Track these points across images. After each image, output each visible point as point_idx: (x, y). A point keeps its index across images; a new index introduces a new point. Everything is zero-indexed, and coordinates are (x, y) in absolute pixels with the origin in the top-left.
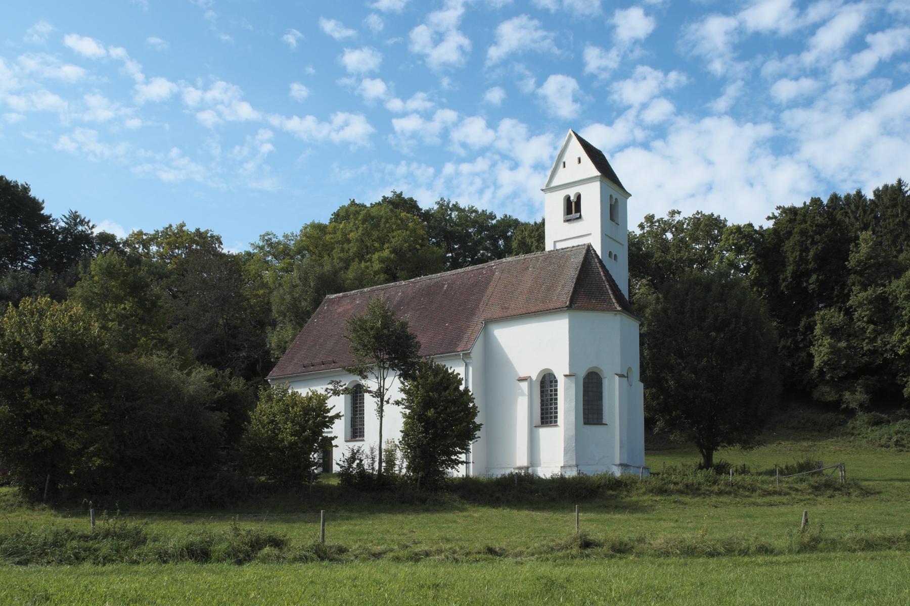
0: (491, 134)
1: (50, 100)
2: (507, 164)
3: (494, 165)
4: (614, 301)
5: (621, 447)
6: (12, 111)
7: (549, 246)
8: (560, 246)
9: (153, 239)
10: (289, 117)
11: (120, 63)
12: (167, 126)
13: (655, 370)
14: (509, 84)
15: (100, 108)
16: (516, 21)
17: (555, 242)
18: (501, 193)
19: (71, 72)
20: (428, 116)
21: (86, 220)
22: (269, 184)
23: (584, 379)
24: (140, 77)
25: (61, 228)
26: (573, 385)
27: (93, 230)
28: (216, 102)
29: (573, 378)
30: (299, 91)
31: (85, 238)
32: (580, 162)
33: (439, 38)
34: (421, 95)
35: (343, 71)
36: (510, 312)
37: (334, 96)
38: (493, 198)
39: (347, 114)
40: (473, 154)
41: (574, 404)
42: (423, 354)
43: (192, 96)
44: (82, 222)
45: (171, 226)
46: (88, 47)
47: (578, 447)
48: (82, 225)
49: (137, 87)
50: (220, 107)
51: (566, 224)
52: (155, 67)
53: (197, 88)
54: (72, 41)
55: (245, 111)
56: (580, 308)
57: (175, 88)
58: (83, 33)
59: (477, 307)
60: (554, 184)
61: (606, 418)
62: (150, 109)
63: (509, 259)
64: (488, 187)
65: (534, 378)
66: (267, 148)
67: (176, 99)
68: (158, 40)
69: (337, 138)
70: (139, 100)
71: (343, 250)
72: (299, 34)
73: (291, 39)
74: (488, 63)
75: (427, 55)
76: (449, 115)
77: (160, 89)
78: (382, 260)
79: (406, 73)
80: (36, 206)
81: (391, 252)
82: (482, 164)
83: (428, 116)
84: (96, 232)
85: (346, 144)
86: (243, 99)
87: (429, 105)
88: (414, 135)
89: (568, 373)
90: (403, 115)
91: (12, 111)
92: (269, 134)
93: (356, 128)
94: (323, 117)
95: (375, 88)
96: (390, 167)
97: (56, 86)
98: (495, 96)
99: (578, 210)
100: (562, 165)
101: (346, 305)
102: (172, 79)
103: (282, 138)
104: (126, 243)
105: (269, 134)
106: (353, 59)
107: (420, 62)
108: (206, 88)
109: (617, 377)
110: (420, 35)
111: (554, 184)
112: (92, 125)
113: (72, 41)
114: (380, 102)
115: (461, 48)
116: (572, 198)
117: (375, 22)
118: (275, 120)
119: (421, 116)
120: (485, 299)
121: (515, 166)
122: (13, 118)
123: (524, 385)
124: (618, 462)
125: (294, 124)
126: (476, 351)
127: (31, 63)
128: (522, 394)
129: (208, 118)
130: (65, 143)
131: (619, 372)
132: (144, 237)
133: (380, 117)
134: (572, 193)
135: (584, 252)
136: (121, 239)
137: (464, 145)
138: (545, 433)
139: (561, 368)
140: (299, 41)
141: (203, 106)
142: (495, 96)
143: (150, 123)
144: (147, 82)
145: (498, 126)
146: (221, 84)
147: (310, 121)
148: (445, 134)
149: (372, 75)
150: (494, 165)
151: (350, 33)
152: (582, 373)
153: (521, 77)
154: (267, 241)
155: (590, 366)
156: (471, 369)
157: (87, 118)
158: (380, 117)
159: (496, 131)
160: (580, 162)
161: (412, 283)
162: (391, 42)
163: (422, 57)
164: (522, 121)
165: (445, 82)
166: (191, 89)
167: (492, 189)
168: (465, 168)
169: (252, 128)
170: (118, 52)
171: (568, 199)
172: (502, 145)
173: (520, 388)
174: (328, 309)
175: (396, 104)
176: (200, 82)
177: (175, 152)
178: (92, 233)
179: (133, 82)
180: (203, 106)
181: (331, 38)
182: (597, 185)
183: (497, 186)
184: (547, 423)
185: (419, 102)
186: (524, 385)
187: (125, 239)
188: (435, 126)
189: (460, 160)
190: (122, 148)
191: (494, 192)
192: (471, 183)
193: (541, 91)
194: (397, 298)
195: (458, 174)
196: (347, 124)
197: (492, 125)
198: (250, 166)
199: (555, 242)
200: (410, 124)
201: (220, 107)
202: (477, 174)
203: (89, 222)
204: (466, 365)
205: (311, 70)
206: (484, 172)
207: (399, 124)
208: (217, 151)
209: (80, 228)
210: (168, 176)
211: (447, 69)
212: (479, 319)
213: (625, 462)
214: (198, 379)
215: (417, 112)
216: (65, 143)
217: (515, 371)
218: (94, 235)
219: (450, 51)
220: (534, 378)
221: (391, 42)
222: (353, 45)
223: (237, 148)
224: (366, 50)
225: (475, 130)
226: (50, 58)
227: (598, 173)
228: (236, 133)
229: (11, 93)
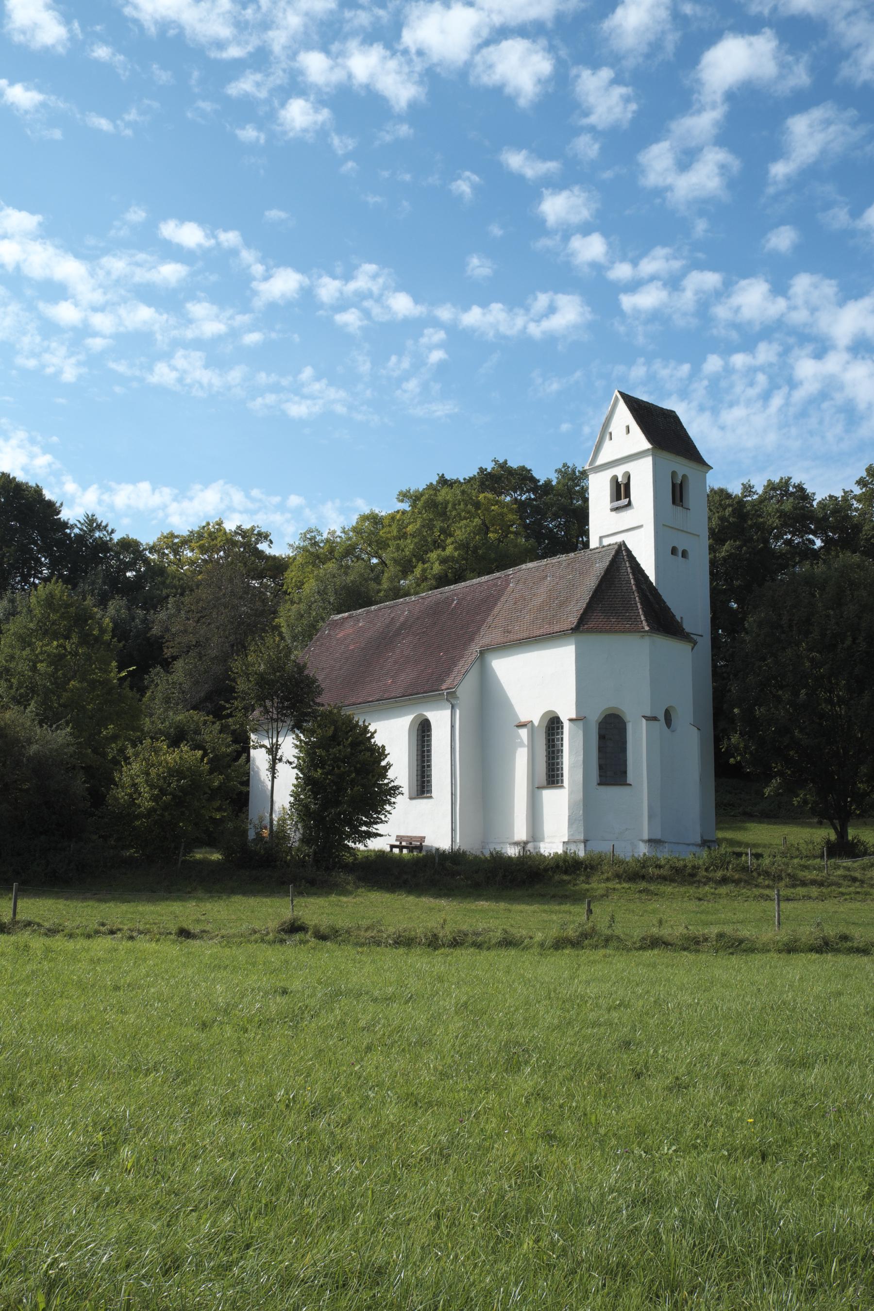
0: (781, 304)
1: (143, 315)
2: (809, 348)
3: (786, 351)
4: (643, 618)
5: (650, 817)
6: (95, 334)
7: (594, 543)
8: (606, 542)
9: (185, 542)
10: (466, 309)
11: (234, 252)
12: (296, 338)
13: (724, 711)
14: (804, 218)
15: (207, 320)
16: (817, 114)
17: (601, 538)
18: (799, 395)
19: (171, 272)
20: (673, 283)
21: (104, 524)
22: (441, 409)
23: (600, 724)
24: (258, 269)
25: (76, 535)
26: (581, 733)
27: (113, 536)
28: (362, 296)
29: (581, 723)
30: (478, 266)
31: (103, 546)
32: (628, 431)
33: (686, 159)
34: (660, 252)
35: (539, 227)
36: (512, 637)
37: (534, 268)
38: (787, 404)
39: (550, 294)
40: (749, 337)
41: (581, 758)
42: (326, 701)
43: (328, 289)
44: (99, 527)
45: (208, 524)
46: (190, 235)
47: (587, 814)
48: (100, 530)
49: (254, 284)
50: (367, 304)
51: (614, 513)
52: (278, 255)
53: (334, 277)
54: (170, 230)
55: (402, 304)
56: (590, 631)
57: (307, 281)
58: (183, 218)
59: (479, 629)
60: (600, 461)
61: (631, 777)
62: (276, 312)
63: (530, 565)
64: (779, 388)
65: (536, 723)
66: (437, 356)
67: (307, 294)
68: (283, 215)
69: (535, 330)
70: (258, 303)
71: (398, 548)
72: (475, 178)
73: (463, 187)
74: (771, 190)
75: (670, 188)
76: (711, 279)
77: (284, 283)
78: (443, 561)
79: (636, 219)
80: (51, 508)
81: (456, 549)
82: (766, 353)
83: (673, 283)
84: (116, 537)
85: (551, 339)
86: (399, 288)
87: (676, 265)
88: (656, 316)
89: (574, 716)
90: (634, 286)
91: (95, 334)
92: (440, 336)
93: (568, 313)
94: (516, 301)
95: (592, 248)
96: (620, 369)
97: (148, 294)
98: (783, 239)
99: (628, 495)
100: (608, 437)
101: (348, 629)
102: (300, 268)
103: (459, 338)
104: (152, 549)
105: (440, 336)
106: (556, 207)
107: (658, 201)
108: (348, 277)
109: (644, 721)
110: (658, 160)
111: (600, 461)
112: (198, 344)
113: (170, 230)
114: (596, 267)
115: (723, 168)
116: (620, 480)
117: (587, 148)
118: (445, 313)
119: (665, 285)
120: (490, 619)
121: (821, 348)
122: (97, 344)
123: (524, 733)
124: (646, 837)
125: (473, 317)
126: (466, 688)
127: (117, 265)
128: (521, 745)
129: (350, 319)
130: (163, 374)
131: (648, 714)
132: (176, 541)
133: (601, 293)
134: (619, 472)
135: (613, 553)
136: (147, 544)
137: (736, 326)
138: (549, 795)
139: (567, 711)
140: (475, 187)
141: (342, 305)
142: (783, 239)
143: (274, 335)
144: (267, 278)
145: (789, 287)
146: (370, 268)
147: (497, 311)
148: (704, 305)
149: (586, 230)
150: (786, 351)
151: (552, 166)
152: (595, 717)
153: (828, 206)
154: (310, 539)
155: (607, 706)
156: (458, 712)
157: (190, 334)
158: (601, 293)
159: (788, 298)
160: (628, 431)
161: (423, 598)
162: (608, 175)
163: (660, 192)
164: (829, 274)
165: (701, 226)
166: (326, 280)
167: (785, 389)
168: (739, 360)
169: (412, 327)
170: (230, 238)
171: (615, 479)
172: (800, 317)
173: (519, 737)
174: (329, 635)
175: (622, 271)
176: (339, 270)
177: (307, 373)
178: (111, 539)
179: (251, 278)
180: (342, 305)
181: (520, 178)
182: (647, 463)
183: (793, 384)
184: (553, 783)
185: (654, 264)
186: (524, 733)
187: (151, 543)
188: (688, 297)
189: (728, 349)
190: (236, 375)
191: (789, 395)
192: (751, 384)
193: (861, 224)
194: (402, 619)
195: (729, 370)
196: (552, 310)
197: (779, 288)
198: (412, 385)
199: (601, 538)
200: (648, 299)
201: (367, 304)
202: (761, 369)
203: (107, 526)
204: (453, 707)
205: (496, 231)
206: (771, 365)
207: (627, 302)
208: (365, 367)
209: (97, 534)
210: (298, 410)
211: (703, 205)
212: (475, 649)
213: (658, 836)
214: (60, 737)
215: (653, 278)
216: (163, 374)
217: (516, 715)
218: (116, 541)
219: (706, 177)
220: (536, 723)
221: (608, 175)
222: (557, 184)
223: (394, 359)
224: (576, 189)
225: (753, 299)
226: (141, 257)
227: (648, 446)
228: (390, 336)
229: (95, 309)
